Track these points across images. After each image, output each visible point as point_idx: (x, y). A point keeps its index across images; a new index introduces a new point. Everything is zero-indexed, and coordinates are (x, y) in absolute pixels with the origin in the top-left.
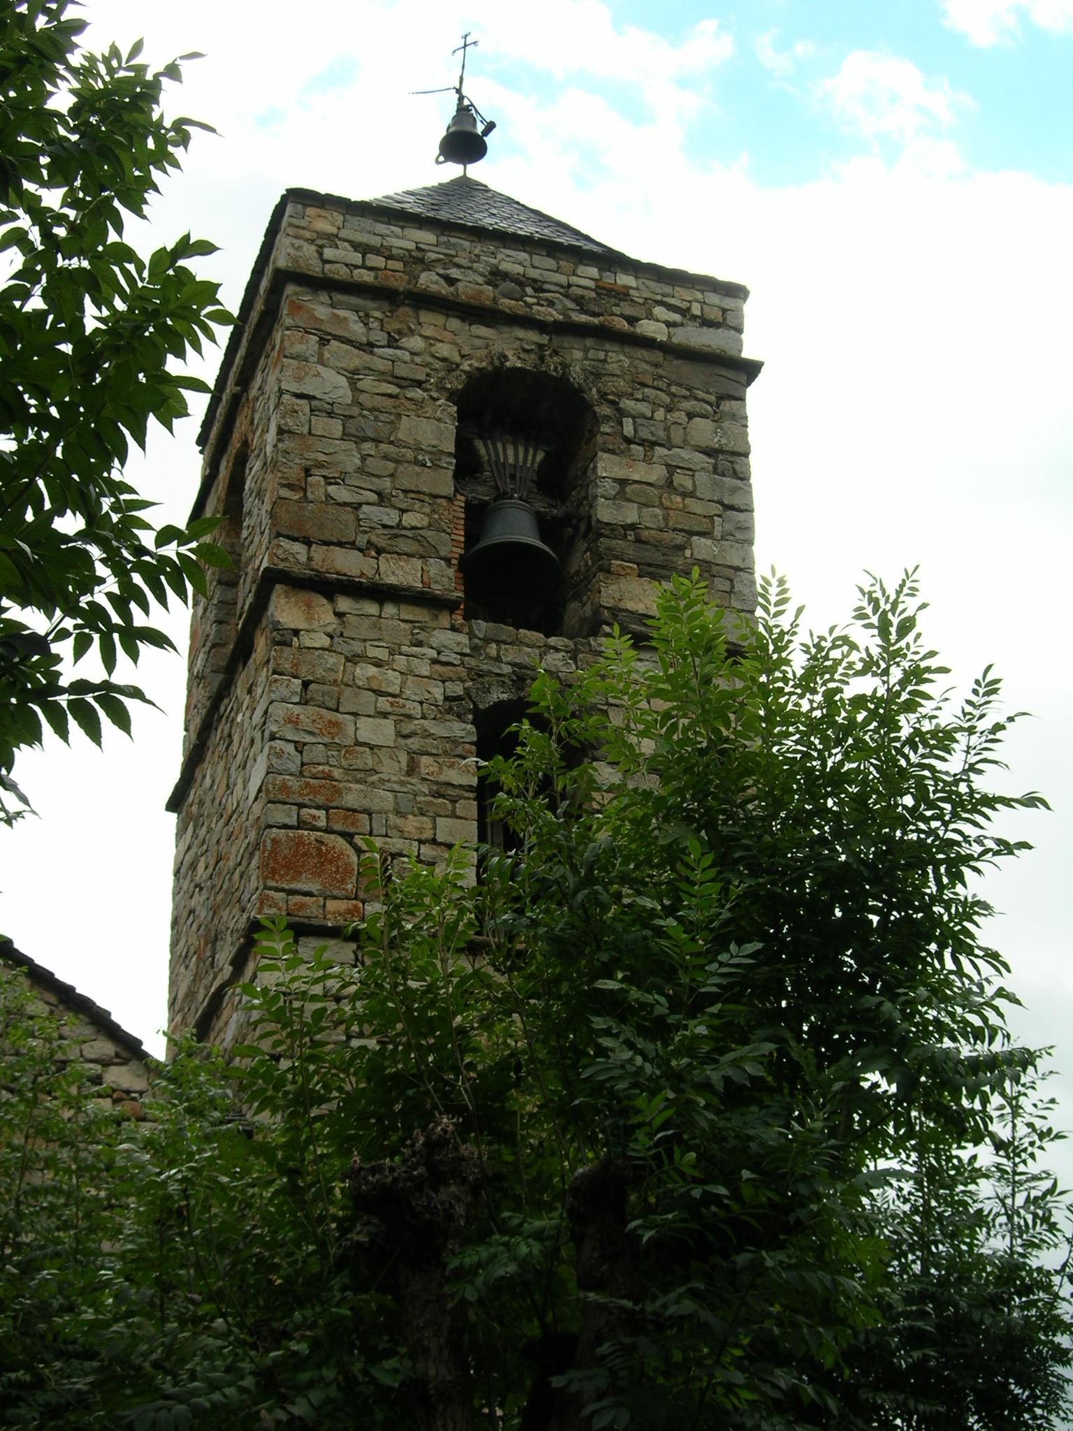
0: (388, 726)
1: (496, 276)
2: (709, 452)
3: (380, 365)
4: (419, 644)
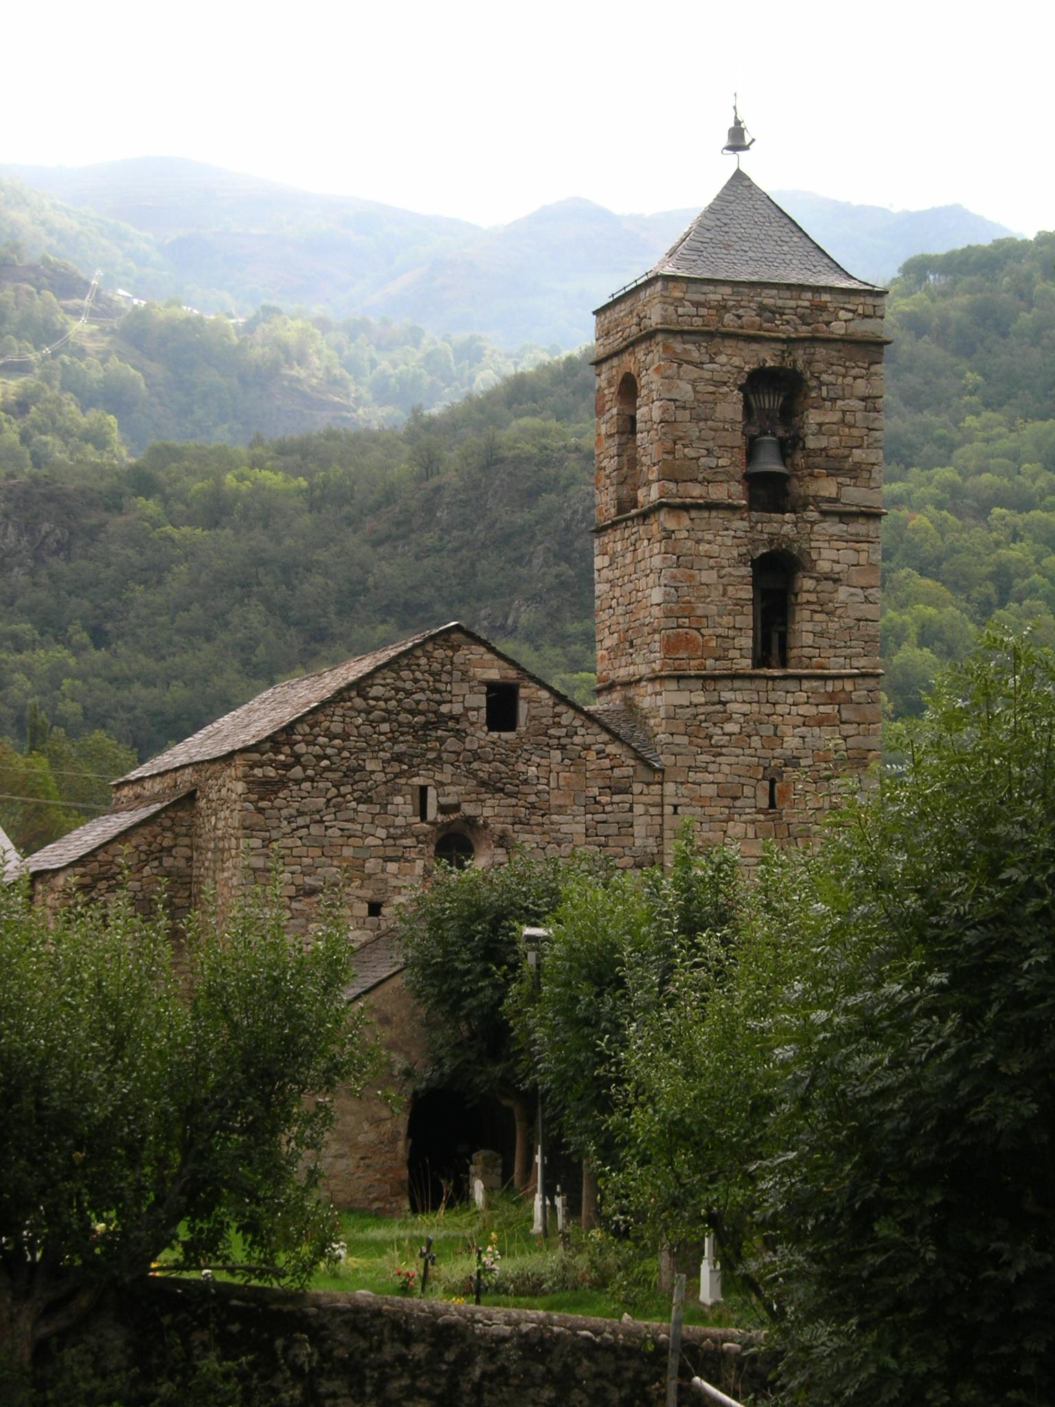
0: (714, 573)
1: (762, 308)
2: (863, 399)
3: (707, 375)
4: (727, 529)
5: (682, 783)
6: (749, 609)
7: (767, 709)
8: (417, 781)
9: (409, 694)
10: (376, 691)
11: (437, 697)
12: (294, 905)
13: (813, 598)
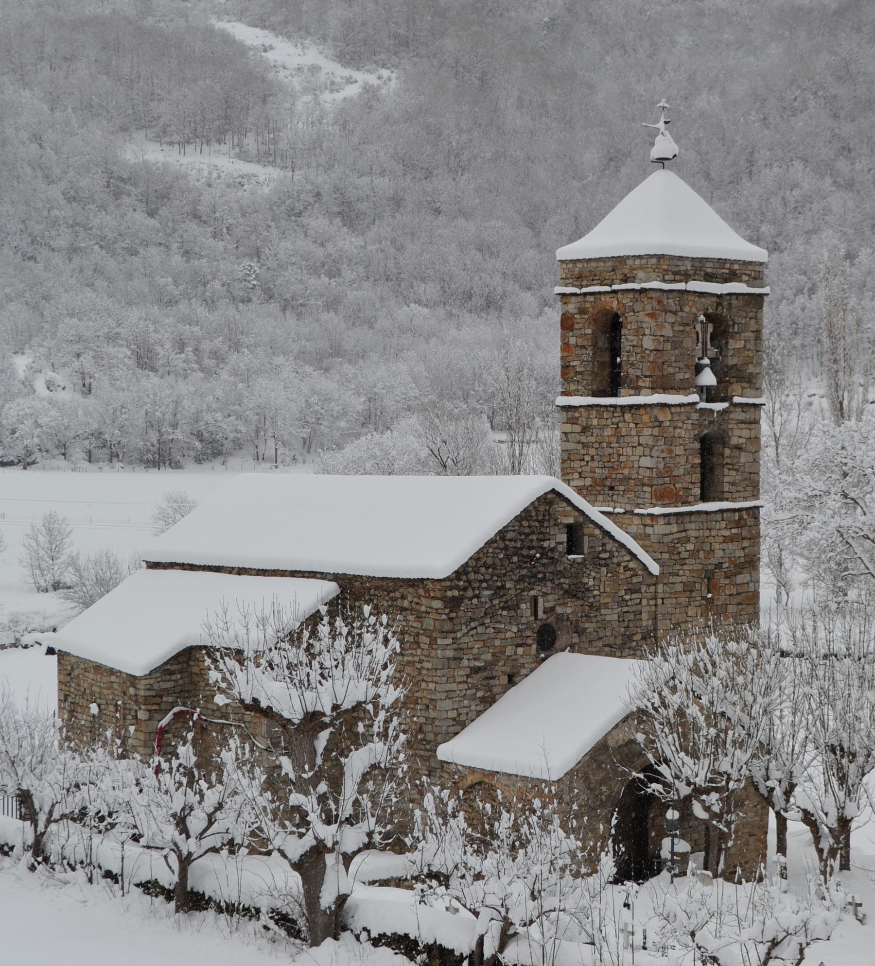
5: (666, 584)
6: (698, 470)
7: (707, 533)
8: (533, 593)
9: (527, 535)
10: (510, 535)
11: (541, 536)
12: (469, 680)
13: (729, 461)
